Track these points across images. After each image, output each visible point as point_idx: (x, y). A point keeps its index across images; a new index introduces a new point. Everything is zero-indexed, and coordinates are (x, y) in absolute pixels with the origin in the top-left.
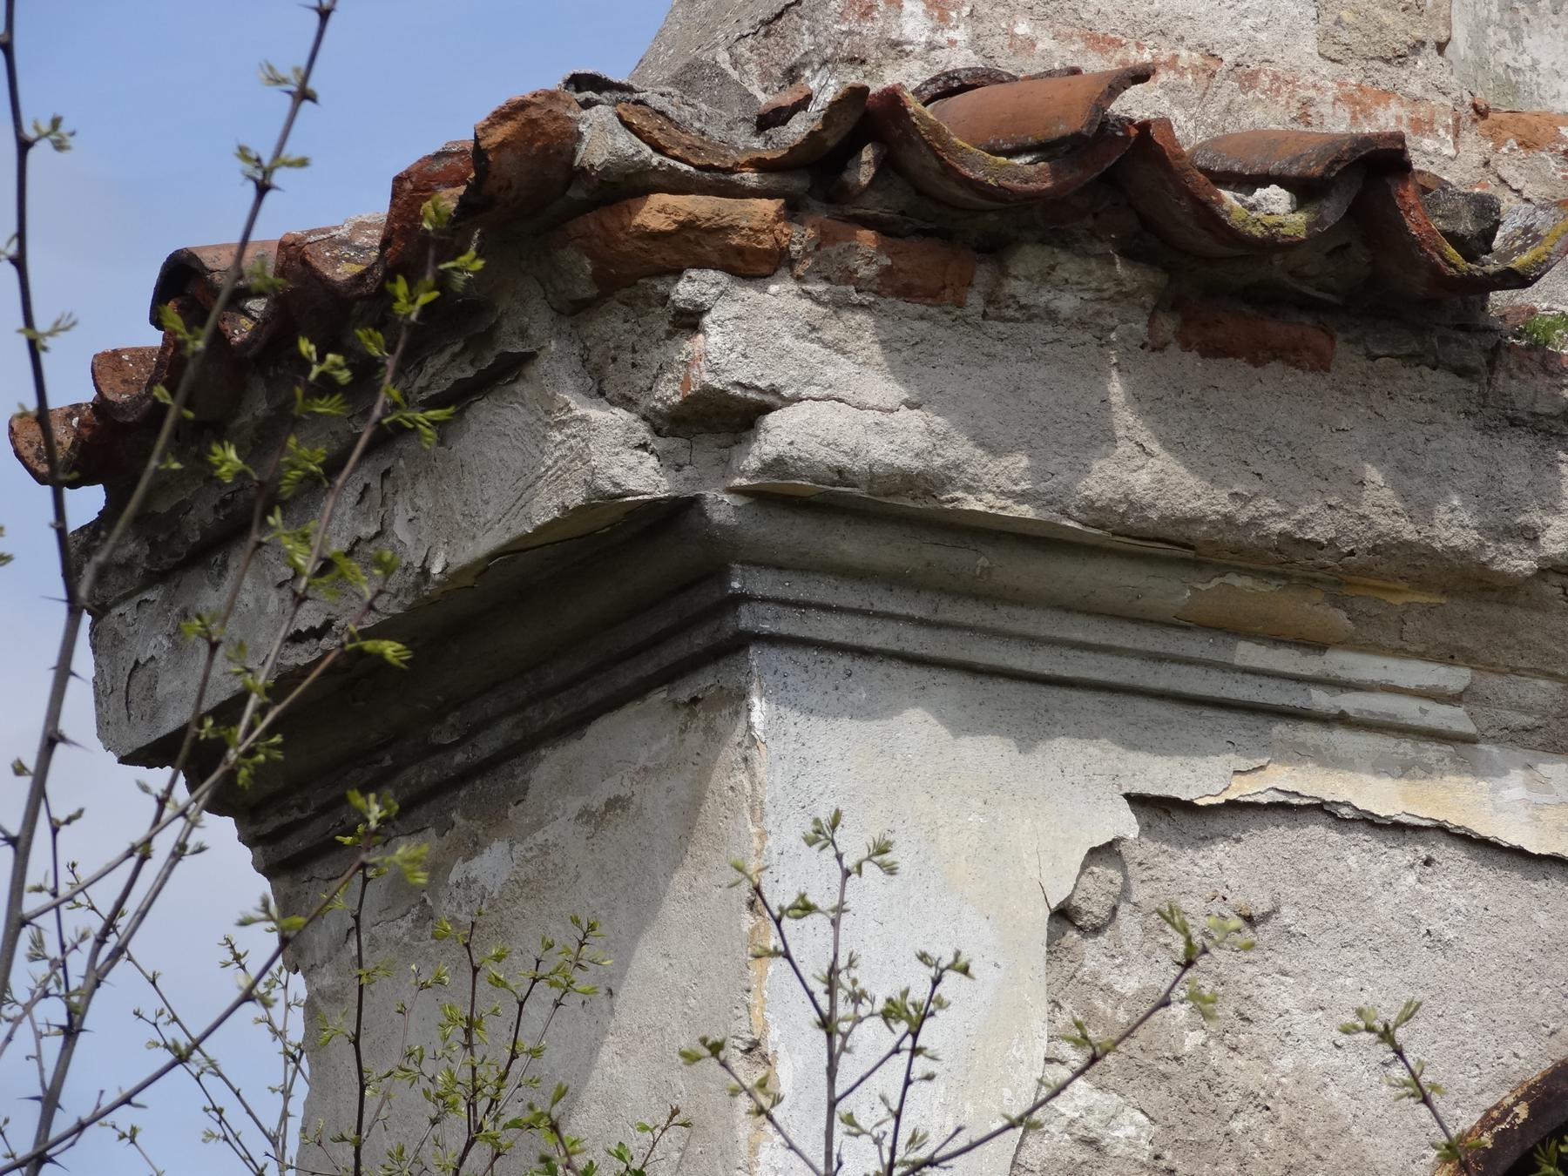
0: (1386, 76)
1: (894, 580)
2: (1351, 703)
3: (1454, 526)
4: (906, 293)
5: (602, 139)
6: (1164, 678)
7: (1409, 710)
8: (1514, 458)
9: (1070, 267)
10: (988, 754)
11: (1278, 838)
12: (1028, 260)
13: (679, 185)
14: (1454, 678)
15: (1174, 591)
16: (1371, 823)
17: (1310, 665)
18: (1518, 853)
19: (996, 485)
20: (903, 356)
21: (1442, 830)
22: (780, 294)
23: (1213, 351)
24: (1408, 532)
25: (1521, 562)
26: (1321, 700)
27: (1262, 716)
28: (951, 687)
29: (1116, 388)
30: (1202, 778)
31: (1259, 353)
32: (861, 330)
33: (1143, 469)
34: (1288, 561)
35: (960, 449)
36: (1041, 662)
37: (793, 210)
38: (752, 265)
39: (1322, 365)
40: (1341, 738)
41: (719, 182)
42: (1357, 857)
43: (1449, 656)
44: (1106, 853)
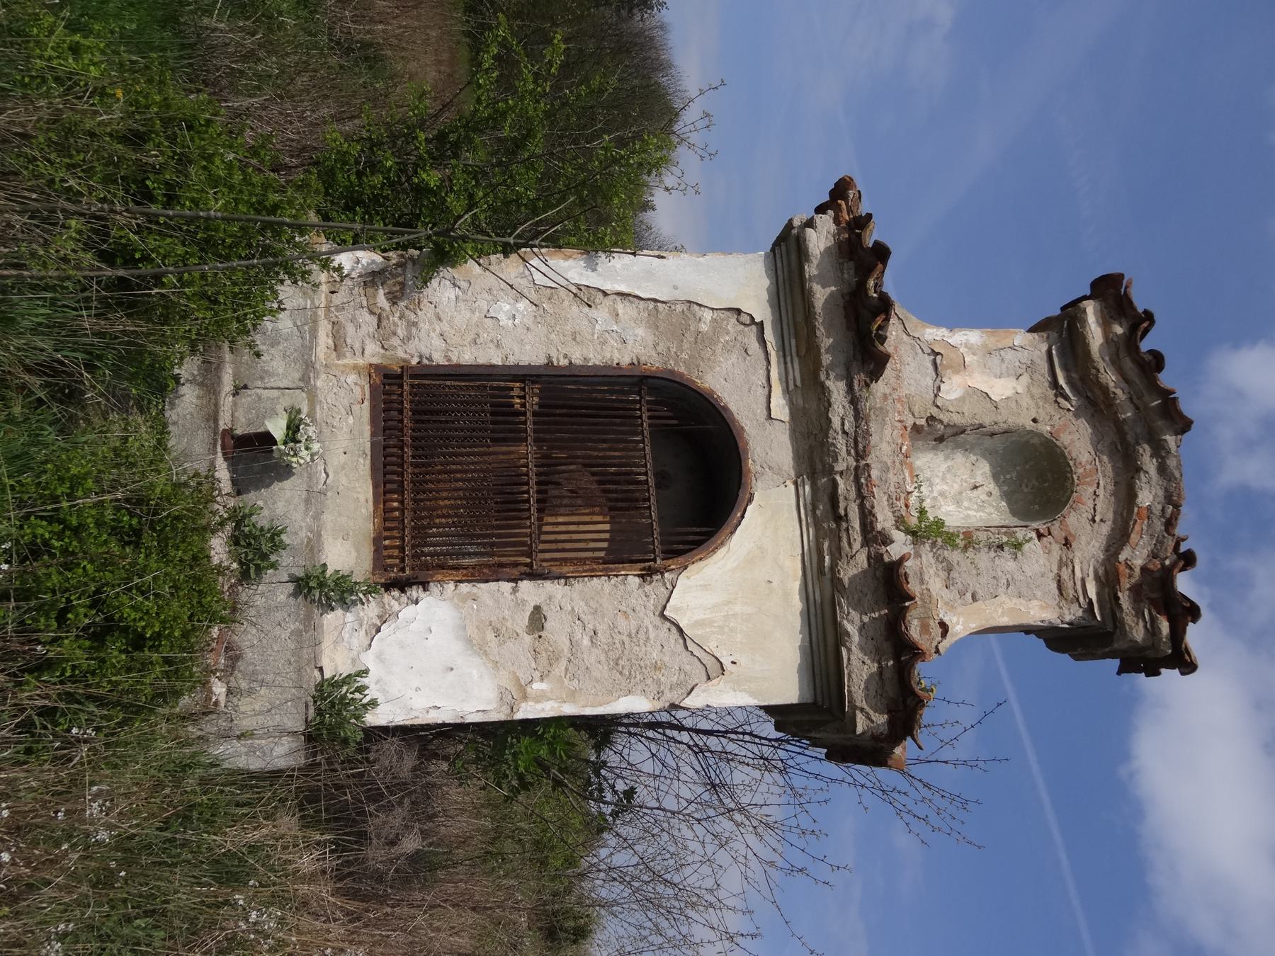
0: (906, 406)
1: (790, 271)
2: (789, 364)
3: (826, 359)
4: (840, 247)
5: (851, 193)
6: (785, 326)
7: (791, 376)
8: (841, 370)
9: (852, 272)
10: (765, 296)
11: (762, 356)
12: (851, 264)
13: (847, 204)
14: (799, 383)
15: (800, 318)
16: (769, 371)
17: (794, 354)
18: (769, 402)
19: (811, 270)
20: (828, 250)
21: (770, 387)
22: (833, 227)
23: (845, 308)
24: (823, 351)
25: (823, 377)
26: (788, 359)
27: (783, 349)
28: (774, 288)
29: (833, 288)
30: (769, 335)
31: (847, 317)
32: (831, 242)
33: (821, 294)
34: (812, 330)
35: (815, 262)
36: (782, 304)
37: (848, 223)
38: (837, 220)
39: (848, 328)
40: (782, 366)
41: (850, 210)
42: (762, 372)
43: (802, 380)
44: (752, 318)
